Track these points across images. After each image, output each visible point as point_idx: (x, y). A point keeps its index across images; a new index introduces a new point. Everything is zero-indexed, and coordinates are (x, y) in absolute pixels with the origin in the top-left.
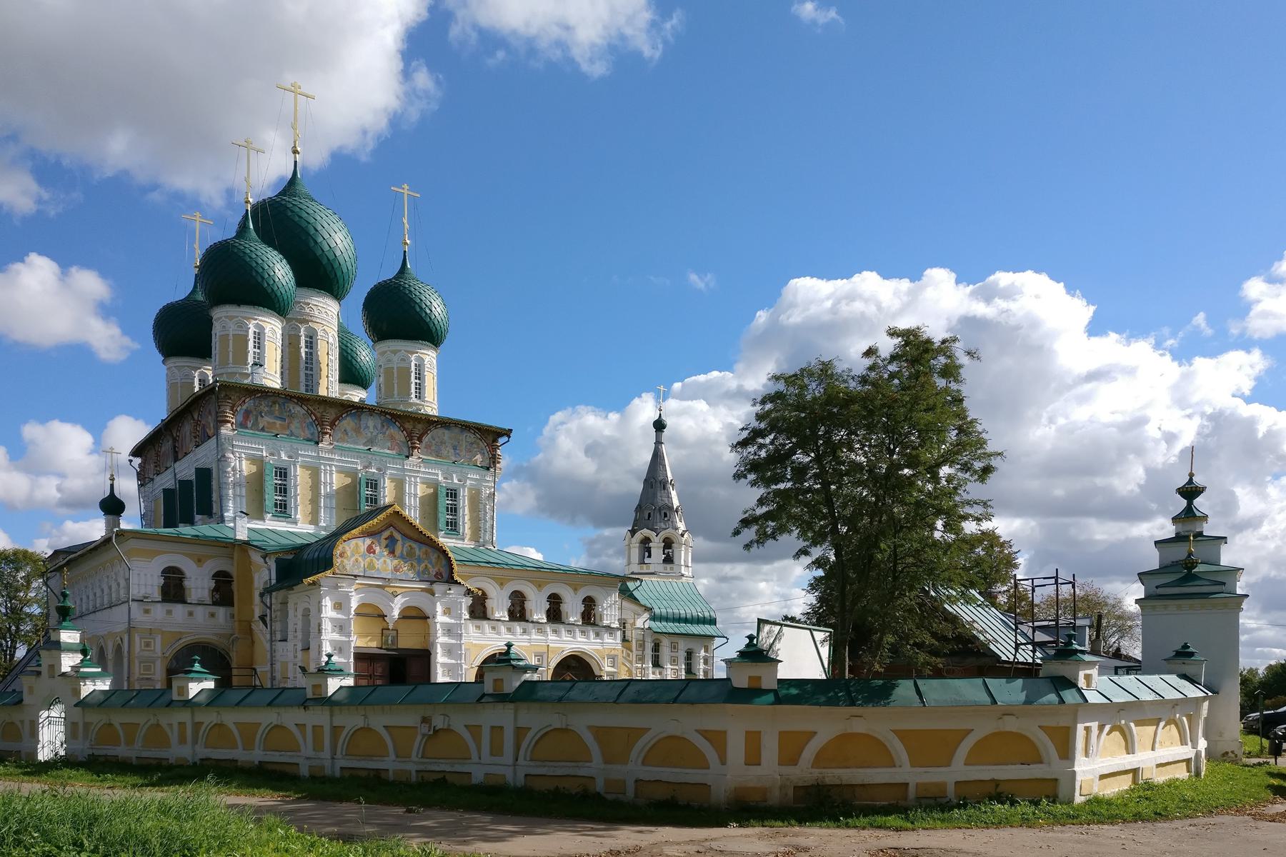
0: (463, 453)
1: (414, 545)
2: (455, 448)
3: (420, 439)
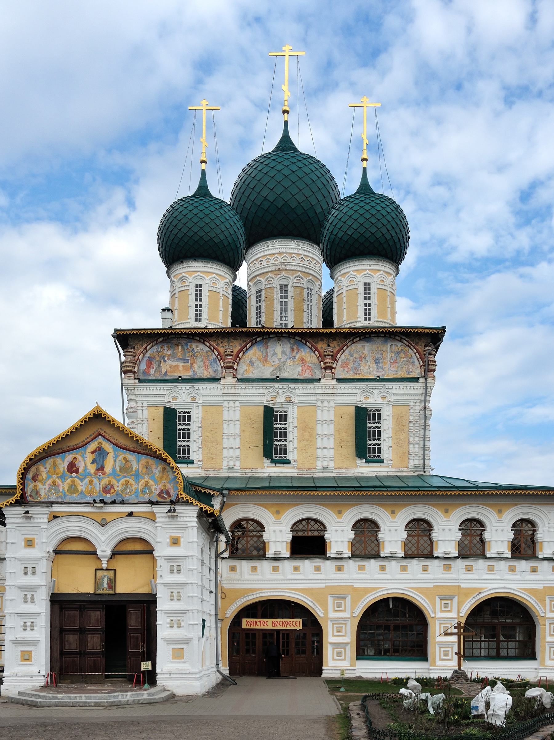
0: (388, 365)
1: (131, 457)
2: (377, 361)
3: (334, 358)
